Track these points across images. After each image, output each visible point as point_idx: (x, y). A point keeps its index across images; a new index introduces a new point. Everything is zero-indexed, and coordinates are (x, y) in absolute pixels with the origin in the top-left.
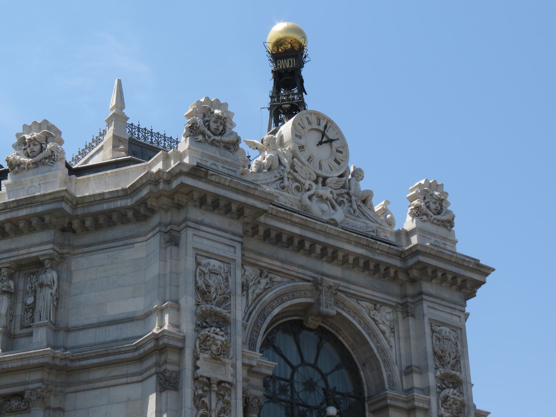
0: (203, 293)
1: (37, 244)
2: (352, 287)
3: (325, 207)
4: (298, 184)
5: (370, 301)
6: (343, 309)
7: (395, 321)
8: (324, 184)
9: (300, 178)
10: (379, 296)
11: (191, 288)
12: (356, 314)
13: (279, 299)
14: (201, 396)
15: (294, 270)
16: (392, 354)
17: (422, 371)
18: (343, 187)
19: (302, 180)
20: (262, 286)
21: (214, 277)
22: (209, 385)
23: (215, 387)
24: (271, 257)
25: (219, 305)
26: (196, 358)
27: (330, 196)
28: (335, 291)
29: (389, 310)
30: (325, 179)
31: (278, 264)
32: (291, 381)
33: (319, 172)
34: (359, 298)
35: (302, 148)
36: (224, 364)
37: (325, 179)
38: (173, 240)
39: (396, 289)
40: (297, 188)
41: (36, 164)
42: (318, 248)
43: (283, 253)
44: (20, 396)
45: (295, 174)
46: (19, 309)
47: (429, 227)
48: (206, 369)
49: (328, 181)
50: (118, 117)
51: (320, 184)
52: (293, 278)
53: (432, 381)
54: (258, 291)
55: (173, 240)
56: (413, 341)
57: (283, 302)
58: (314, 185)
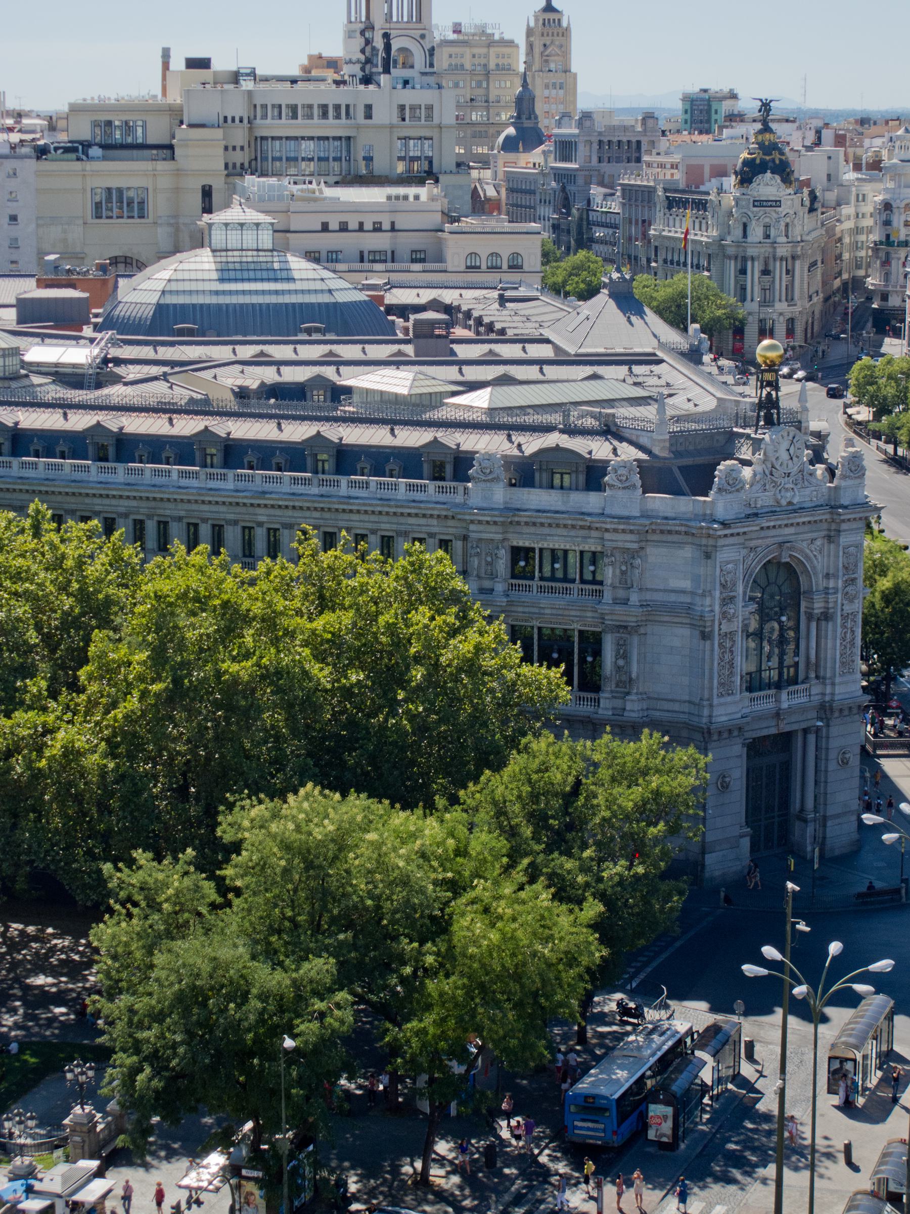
0: (723, 586)
1: (628, 541)
3: (789, 494)
7: (823, 545)
10: (815, 535)
11: (718, 586)
12: (801, 551)
16: (819, 567)
17: (836, 577)
38: (708, 556)
41: (624, 488)
44: (626, 627)
46: (618, 572)
48: (724, 628)
53: (840, 584)
55: (708, 556)
56: (832, 558)
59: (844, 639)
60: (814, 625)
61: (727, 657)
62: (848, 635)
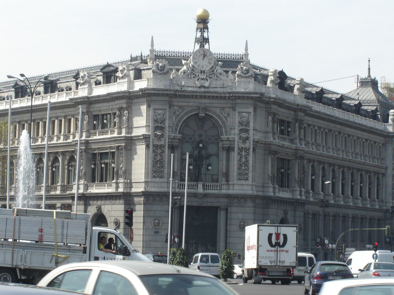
2: (213, 105)
4: (194, 76)
5: (220, 107)
6: (209, 112)
8: (204, 73)
9: (195, 73)
12: (215, 113)
13: (186, 114)
14: (154, 150)
15: (191, 104)
18: (213, 71)
19: (196, 74)
20: (180, 112)
21: (159, 116)
22: (157, 146)
23: (159, 147)
24: (184, 102)
25: (161, 123)
26: (154, 140)
27: (205, 77)
28: (205, 109)
29: (227, 109)
30: (204, 71)
31: (186, 103)
32: (194, 136)
33: (202, 69)
34: (216, 107)
35: (196, 63)
36: (162, 140)
37: (204, 71)
39: (230, 102)
40: (194, 77)
42: (198, 97)
43: (187, 100)
45: (193, 72)
47: (243, 79)
49: (205, 72)
50: (152, 51)
51: (203, 73)
52: (192, 106)
54: (178, 114)
57: (187, 115)
58: (200, 74)
59: (240, 160)
60: (225, 153)
61: (159, 157)
62: (243, 160)
